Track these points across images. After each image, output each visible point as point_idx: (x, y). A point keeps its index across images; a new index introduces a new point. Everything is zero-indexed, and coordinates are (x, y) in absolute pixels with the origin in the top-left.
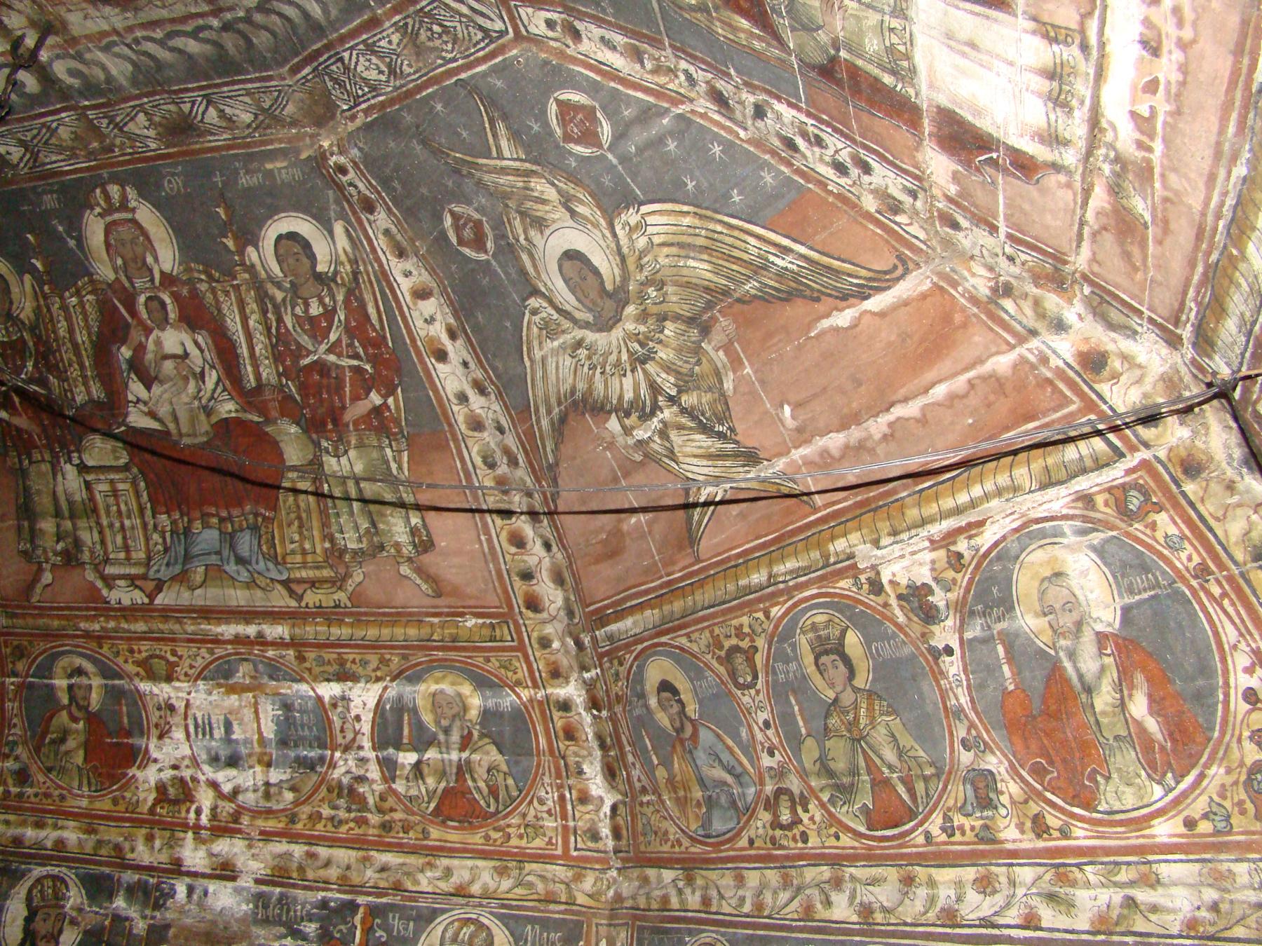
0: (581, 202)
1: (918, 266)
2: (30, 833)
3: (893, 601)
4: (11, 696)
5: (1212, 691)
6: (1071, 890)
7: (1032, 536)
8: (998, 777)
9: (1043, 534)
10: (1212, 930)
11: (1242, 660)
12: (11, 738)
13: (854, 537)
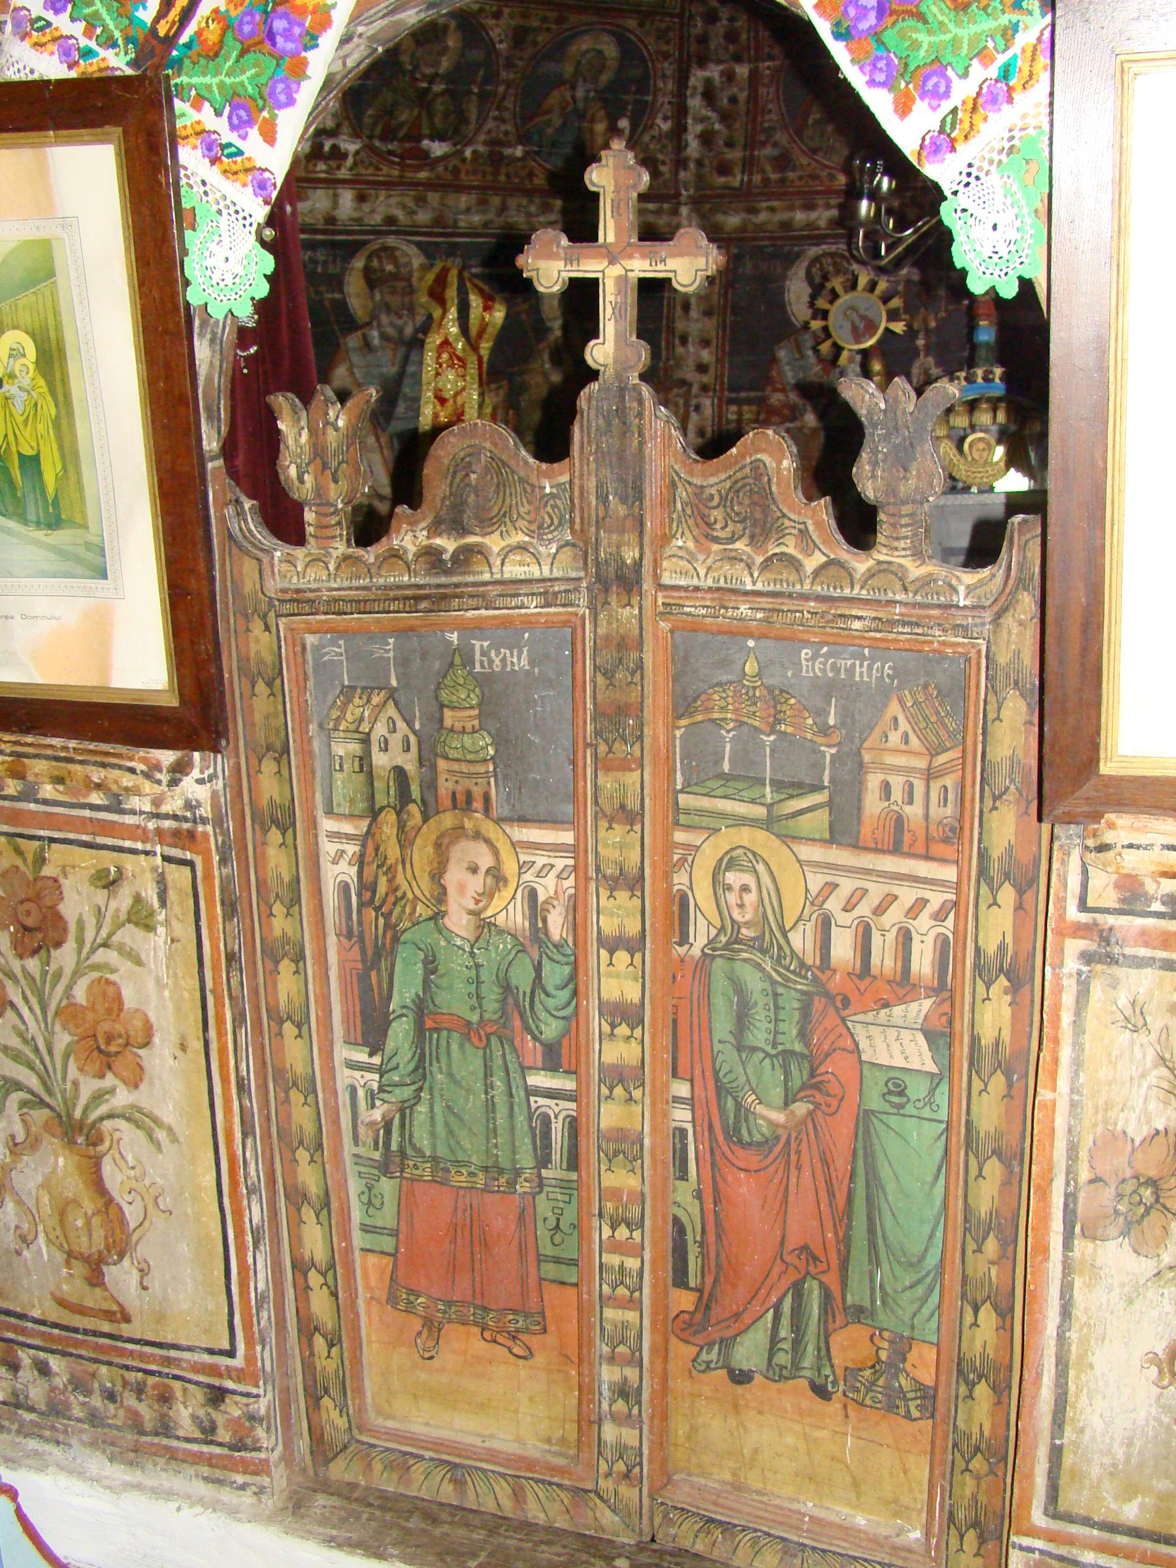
2: (800, 216)
4: (766, 81)
12: (766, 125)
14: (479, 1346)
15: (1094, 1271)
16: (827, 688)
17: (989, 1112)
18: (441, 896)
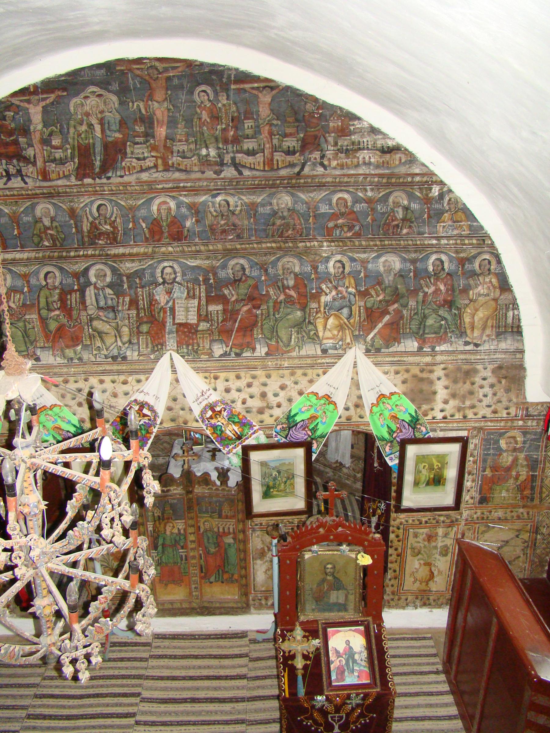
14: (173, 586)
15: (256, 563)
16: (216, 502)
17: (241, 547)
18: (165, 530)
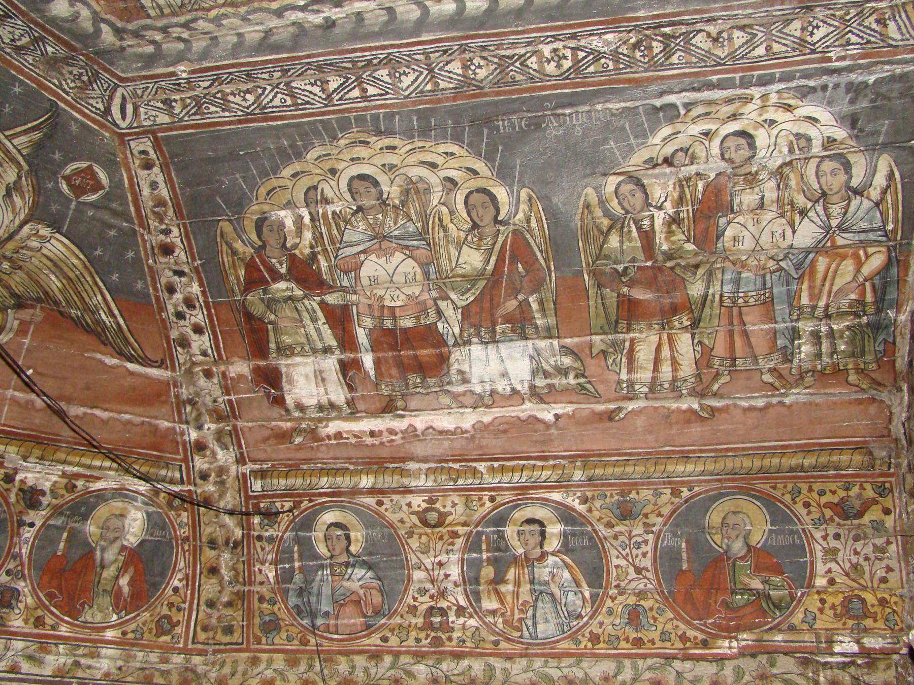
0: (23, 197)
1: (167, 368)
3: (14, 491)
5: (161, 584)
6: (43, 655)
7: (121, 495)
8: (22, 594)
9: (126, 496)
10: (117, 678)
11: (180, 576)
13: (12, 449)
